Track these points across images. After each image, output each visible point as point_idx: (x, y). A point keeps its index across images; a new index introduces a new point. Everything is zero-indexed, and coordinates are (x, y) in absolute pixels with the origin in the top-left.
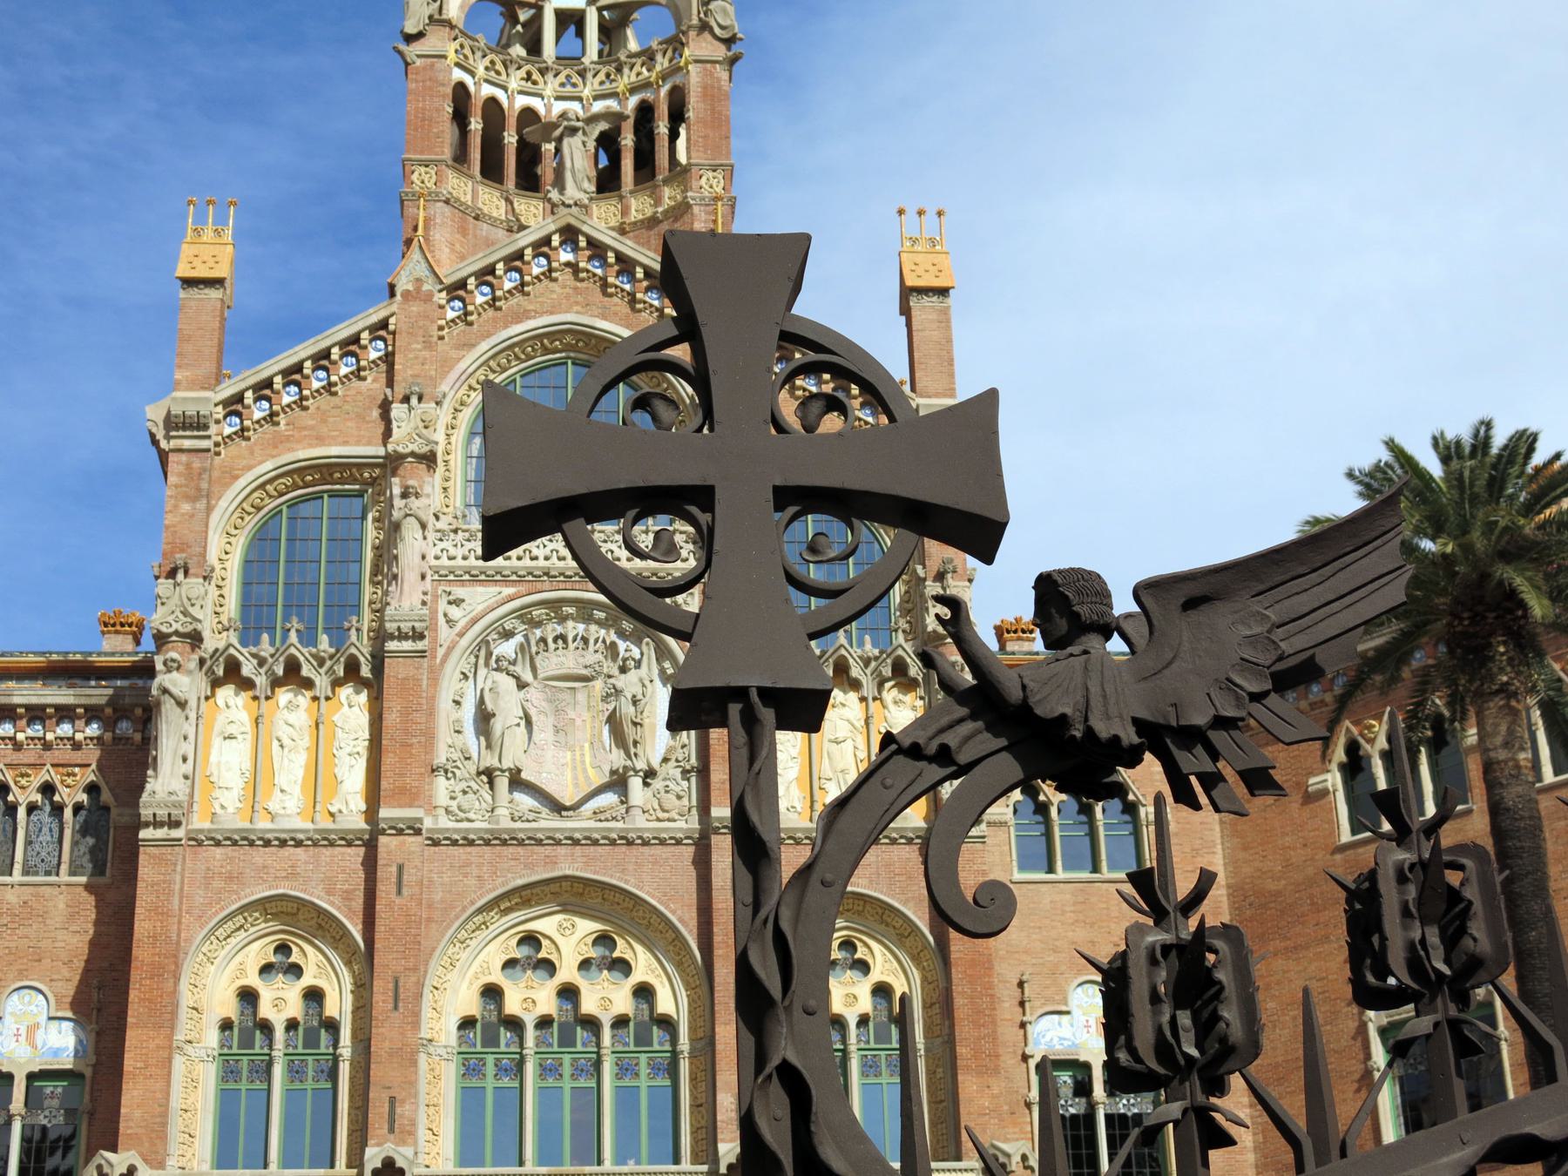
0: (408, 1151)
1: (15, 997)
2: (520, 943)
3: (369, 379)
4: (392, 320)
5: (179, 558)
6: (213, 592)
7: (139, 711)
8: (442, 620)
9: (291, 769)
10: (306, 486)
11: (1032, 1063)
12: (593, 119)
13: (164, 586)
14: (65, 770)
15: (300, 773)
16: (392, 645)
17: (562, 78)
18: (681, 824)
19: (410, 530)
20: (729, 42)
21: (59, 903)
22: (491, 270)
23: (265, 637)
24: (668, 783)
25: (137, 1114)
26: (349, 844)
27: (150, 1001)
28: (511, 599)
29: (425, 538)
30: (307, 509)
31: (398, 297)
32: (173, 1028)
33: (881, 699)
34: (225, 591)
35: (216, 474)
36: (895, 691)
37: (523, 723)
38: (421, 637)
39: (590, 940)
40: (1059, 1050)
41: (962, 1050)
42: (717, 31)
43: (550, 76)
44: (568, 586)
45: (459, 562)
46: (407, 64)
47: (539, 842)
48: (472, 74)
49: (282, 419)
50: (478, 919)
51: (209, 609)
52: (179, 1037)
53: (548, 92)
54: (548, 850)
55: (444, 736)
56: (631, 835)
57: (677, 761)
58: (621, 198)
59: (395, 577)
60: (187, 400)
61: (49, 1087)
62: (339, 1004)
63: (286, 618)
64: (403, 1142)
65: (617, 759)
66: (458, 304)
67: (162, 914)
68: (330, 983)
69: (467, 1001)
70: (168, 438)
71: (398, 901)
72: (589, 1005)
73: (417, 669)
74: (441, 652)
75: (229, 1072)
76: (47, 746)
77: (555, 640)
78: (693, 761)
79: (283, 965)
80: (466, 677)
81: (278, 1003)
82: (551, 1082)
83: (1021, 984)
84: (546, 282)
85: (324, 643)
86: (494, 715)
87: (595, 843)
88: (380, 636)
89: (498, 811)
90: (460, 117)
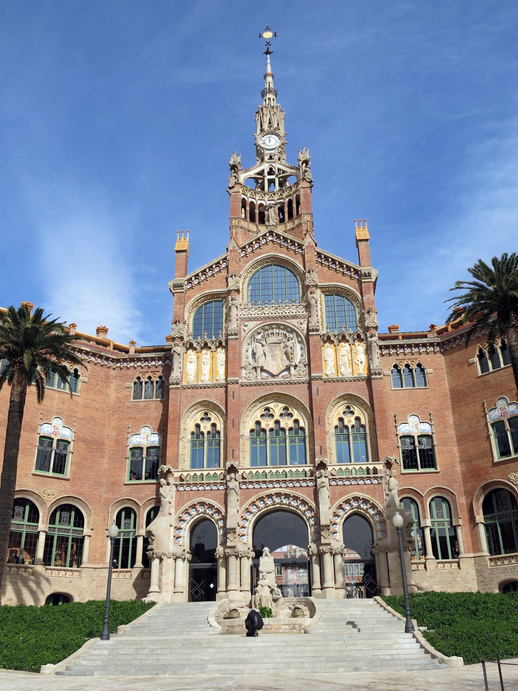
0: (237, 463)
1: (143, 429)
2: (265, 410)
5: (177, 319)
6: (186, 327)
9: (206, 369)
11: (399, 436)
12: (276, 204)
15: (208, 370)
16: (230, 337)
17: (269, 195)
18: (304, 378)
19: (234, 309)
20: (310, 182)
21: (153, 405)
22: (252, 243)
23: (199, 337)
25: (171, 455)
26: (221, 387)
28: (259, 324)
30: (208, 305)
32: (179, 434)
34: (189, 327)
35: (186, 298)
36: (358, 342)
38: (237, 335)
39: (282, 409)
41: (378, 433)
42: (307, 180)
43: (266, 195)
45: (246, 316)
47: (268, 385)
48: (246, 196)
49: (201, 283)
50: (254, 404)
51: (185, 331)
53: (266, 199)
55: (244, 359)
56: (291, 382)
59: (230, 320)
61: (152, 450)
62: (220, 427)
63: (204, 332)
64: (236, 461)
65: (287, 363)
66: (244, 252)
69: (252, 425)
72: (282, 425)
74: (242, 338)
75: (194, 445)
76: (149, 367)
77: (271, 334)
78: (307, 362)
79: (206, 418)
80: (249, 344)
82: (274, 445)
83: (395, 416)
85: (214, 338)
87: (282, 384)
88: (227, 335)
90: (244, 206)
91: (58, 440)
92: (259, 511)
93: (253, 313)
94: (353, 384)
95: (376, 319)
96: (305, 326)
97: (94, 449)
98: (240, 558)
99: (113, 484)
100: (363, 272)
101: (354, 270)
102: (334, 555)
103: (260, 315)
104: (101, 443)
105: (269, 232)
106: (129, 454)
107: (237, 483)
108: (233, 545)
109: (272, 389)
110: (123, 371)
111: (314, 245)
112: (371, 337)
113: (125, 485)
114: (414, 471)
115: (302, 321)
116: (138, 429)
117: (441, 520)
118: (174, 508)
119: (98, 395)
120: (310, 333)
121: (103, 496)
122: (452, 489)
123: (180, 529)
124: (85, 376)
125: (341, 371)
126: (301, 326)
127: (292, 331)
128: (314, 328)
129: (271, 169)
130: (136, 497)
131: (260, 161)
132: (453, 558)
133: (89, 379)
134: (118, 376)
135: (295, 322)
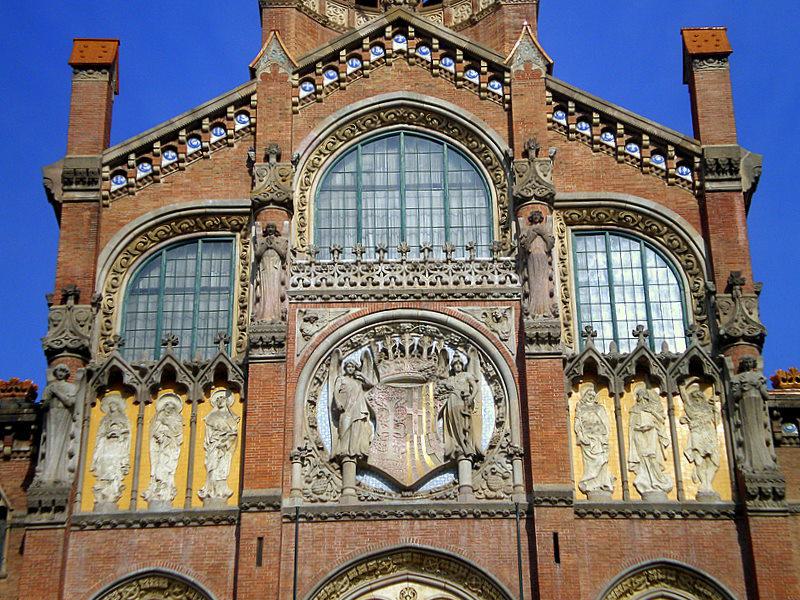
3: (236, 146)
8: (298, 333)
10: (184, 232)
16: (256, 353)
24: (494, 466)
29: (284, 268)
31: (259, 79)
33: (680, 394)
34: (112, 318)
38: (281, 345)
47: (384, 518)
51: (97, 333)
54: (392, 525)
56: (463, 510)
57: (502, 448)
60: (81, 157)
67: (44, 590)
71: (257, 571)
73: (277, 372)
74: (297, 361)
78: (518, 443)
86: (343, 411)
89: (347, 491)
93: (336, 281)
94: (678, 528)
95: (755, 312)
96: (510, 326)
101: (679, 150)
105: (393, 24)
111: (544, 71)
112: (743, 367)
115: (500, 309)
125: (636, 483)
126: (497, 327)
127: (467, 341)
135: (475, 312)
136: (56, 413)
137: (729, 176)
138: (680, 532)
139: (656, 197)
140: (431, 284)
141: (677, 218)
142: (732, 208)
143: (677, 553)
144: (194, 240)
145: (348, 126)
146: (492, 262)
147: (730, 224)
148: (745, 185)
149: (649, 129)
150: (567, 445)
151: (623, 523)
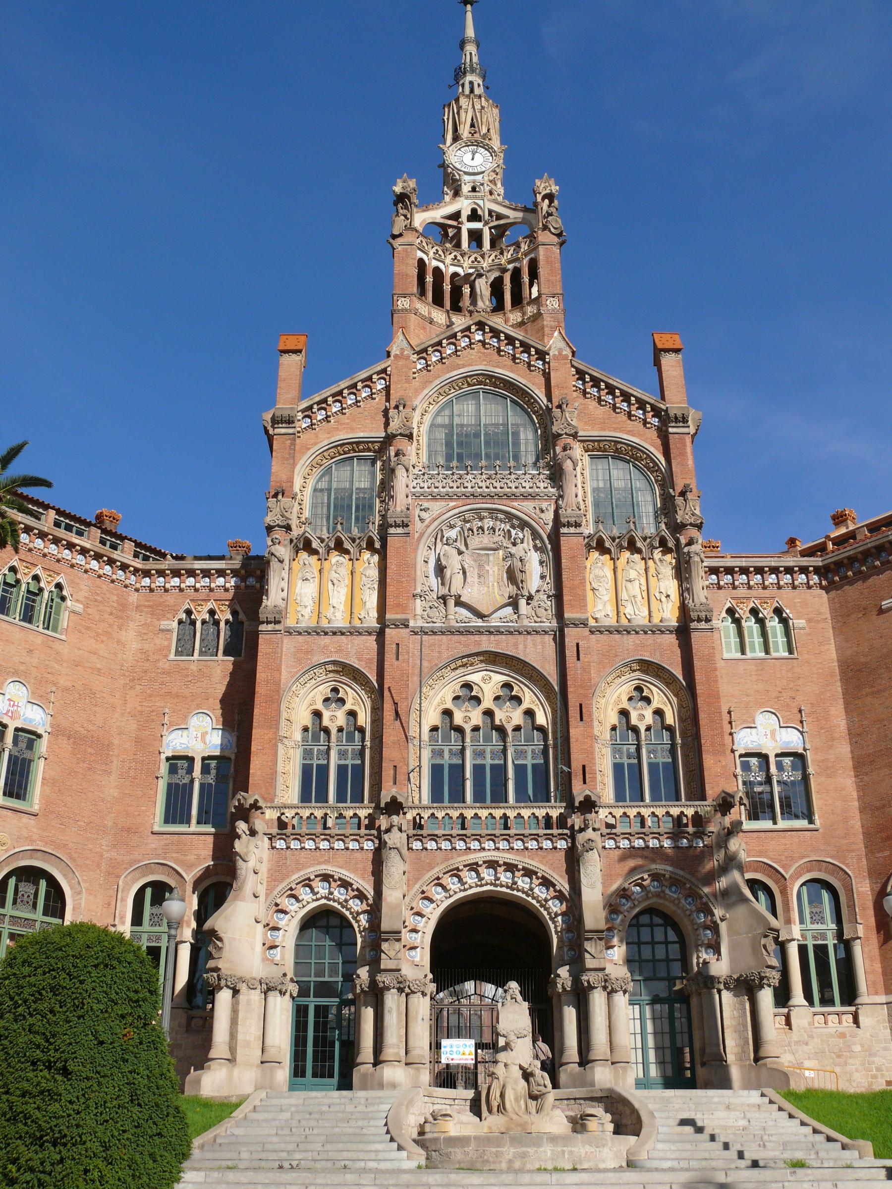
1: (195, 718)
2: (462, 686)
4: (389, 369)
6: (296, 508)
7: (258, 572)
8: (417, 518)
9: (339, 597)
10: (345, 453)
13: (272, 501)
14: (221, 603)
15: (343, 598)
19: (400, 472)
20: (559, 235)
25: (259, 773)
27: (265, 715)
31: (392, 358)
32: (278, 729)
37: (461, 572)
38: (407, 526)
40: (752, 747)
42: (553, 230)
43: (466, 258)
44: (484, 501)
46: (394, 249)
47: (471, 633)
48: (427, 255)
49: (332, 419)
52: (281, 733)
54: (477, 638)
58: (505, 314)
62: (364, 719)
68: (360, 709)
70: (272, 426)
71: (396, 663)
74: (417, 535)
75: (307, 754)
76: (211, 590)
81: (333, 718)
83: (729, 712)
84: (468, 350)
85: (355, 532)
91: (17, 730)
92: (477, 886)
94: (650, 639)
95: (698, 508)
96: (549, 516)
97: (91, 754)
98: (407, 995)
99: (128, 830)
100: (672, 413)
102: (611, 993)
103: (455, 489)
104: (106, 743)
105: (477, 324)
106: (164, 768)
107: (404, 835)
108: (394, 967)
109: (479, 643)
110: (155, 596)
111: (570, 355)
112: (690, 543)
113: (153, 833)
114: (767, 824)
115: (544, 505)
116: (185, 718)
117: (820, 926)
118: (265, 884)
119: (103, 642)
120: (564, 530)
121: (106, 855)
122: (843, 863)
123: (276, 929)
124: (77, 601)
126: (542, 515)
127: (523, 525)
128: (572, 520)
129: (474, 211)
130: (176, 861)
131: (451, 193)
132: (843, 1003)
133: (86, 606)
134: (145, 606)
135: (528, 506)
136: (274, 564)
137: (681, 424)
138: (651, 641)
139: (639, 435)
140: (501, 488)
141: (652, 449)
142: (684, 445)
143: (648, 654)
144: (352, 458)
145: (447, 387)
146: (539, 474)
147: (683, 454)
148: (692, 430)
149: (635, 393)
150: (585, 590)
151: (617, 636)
